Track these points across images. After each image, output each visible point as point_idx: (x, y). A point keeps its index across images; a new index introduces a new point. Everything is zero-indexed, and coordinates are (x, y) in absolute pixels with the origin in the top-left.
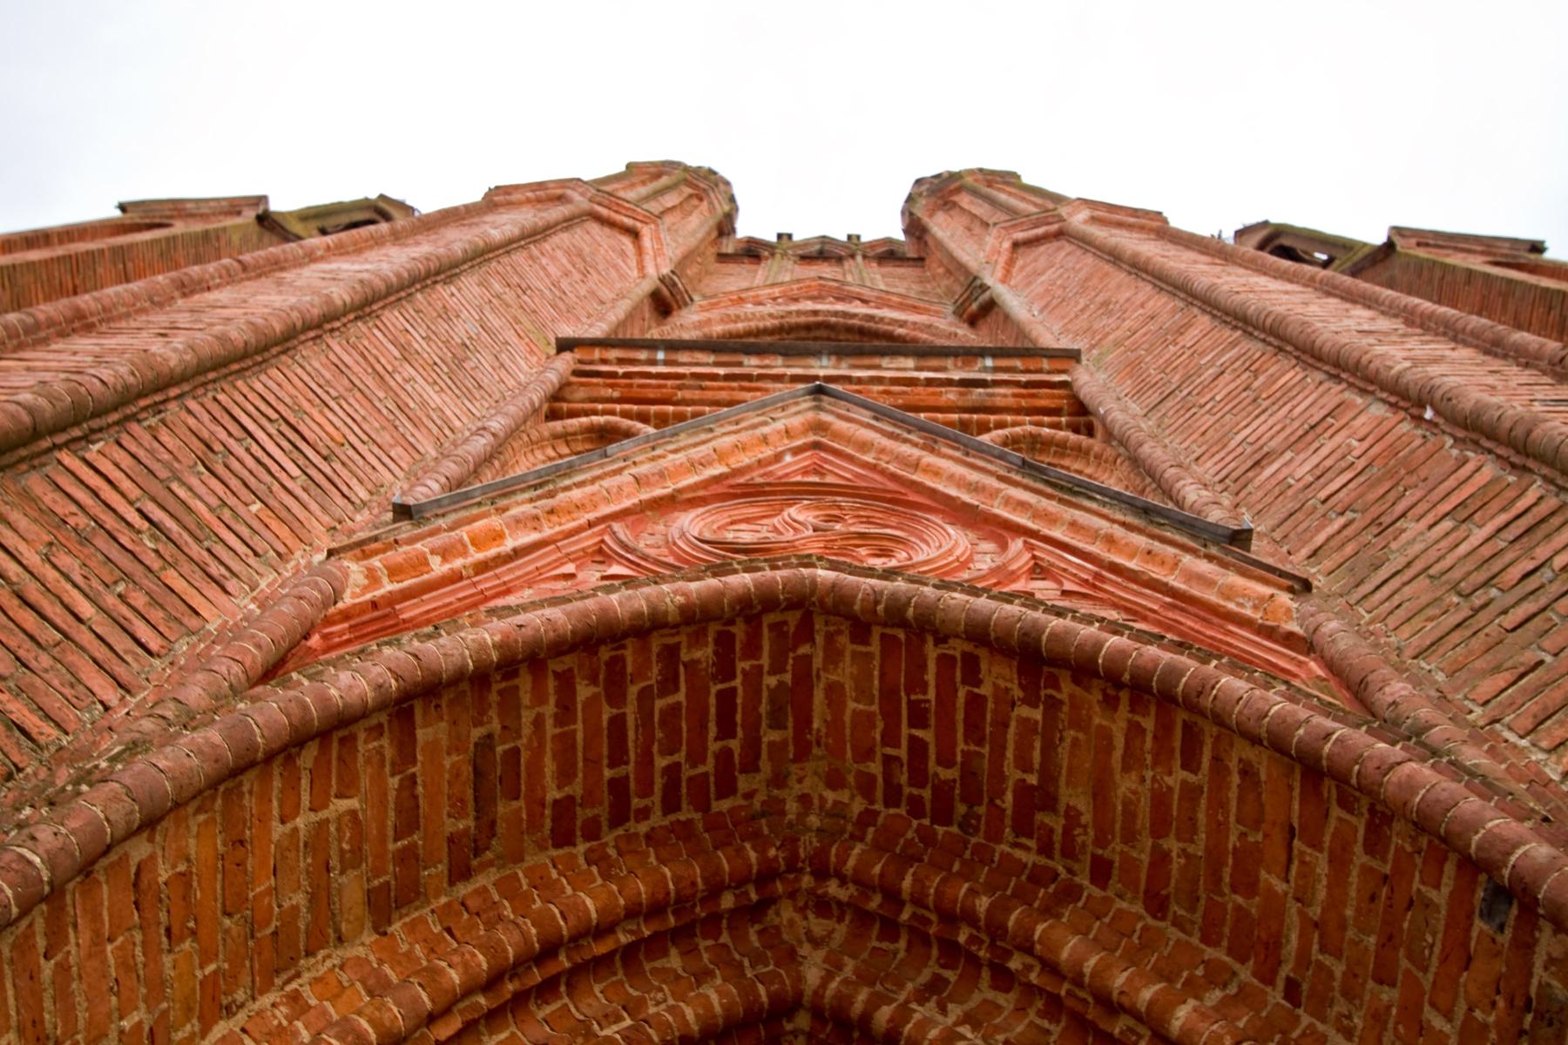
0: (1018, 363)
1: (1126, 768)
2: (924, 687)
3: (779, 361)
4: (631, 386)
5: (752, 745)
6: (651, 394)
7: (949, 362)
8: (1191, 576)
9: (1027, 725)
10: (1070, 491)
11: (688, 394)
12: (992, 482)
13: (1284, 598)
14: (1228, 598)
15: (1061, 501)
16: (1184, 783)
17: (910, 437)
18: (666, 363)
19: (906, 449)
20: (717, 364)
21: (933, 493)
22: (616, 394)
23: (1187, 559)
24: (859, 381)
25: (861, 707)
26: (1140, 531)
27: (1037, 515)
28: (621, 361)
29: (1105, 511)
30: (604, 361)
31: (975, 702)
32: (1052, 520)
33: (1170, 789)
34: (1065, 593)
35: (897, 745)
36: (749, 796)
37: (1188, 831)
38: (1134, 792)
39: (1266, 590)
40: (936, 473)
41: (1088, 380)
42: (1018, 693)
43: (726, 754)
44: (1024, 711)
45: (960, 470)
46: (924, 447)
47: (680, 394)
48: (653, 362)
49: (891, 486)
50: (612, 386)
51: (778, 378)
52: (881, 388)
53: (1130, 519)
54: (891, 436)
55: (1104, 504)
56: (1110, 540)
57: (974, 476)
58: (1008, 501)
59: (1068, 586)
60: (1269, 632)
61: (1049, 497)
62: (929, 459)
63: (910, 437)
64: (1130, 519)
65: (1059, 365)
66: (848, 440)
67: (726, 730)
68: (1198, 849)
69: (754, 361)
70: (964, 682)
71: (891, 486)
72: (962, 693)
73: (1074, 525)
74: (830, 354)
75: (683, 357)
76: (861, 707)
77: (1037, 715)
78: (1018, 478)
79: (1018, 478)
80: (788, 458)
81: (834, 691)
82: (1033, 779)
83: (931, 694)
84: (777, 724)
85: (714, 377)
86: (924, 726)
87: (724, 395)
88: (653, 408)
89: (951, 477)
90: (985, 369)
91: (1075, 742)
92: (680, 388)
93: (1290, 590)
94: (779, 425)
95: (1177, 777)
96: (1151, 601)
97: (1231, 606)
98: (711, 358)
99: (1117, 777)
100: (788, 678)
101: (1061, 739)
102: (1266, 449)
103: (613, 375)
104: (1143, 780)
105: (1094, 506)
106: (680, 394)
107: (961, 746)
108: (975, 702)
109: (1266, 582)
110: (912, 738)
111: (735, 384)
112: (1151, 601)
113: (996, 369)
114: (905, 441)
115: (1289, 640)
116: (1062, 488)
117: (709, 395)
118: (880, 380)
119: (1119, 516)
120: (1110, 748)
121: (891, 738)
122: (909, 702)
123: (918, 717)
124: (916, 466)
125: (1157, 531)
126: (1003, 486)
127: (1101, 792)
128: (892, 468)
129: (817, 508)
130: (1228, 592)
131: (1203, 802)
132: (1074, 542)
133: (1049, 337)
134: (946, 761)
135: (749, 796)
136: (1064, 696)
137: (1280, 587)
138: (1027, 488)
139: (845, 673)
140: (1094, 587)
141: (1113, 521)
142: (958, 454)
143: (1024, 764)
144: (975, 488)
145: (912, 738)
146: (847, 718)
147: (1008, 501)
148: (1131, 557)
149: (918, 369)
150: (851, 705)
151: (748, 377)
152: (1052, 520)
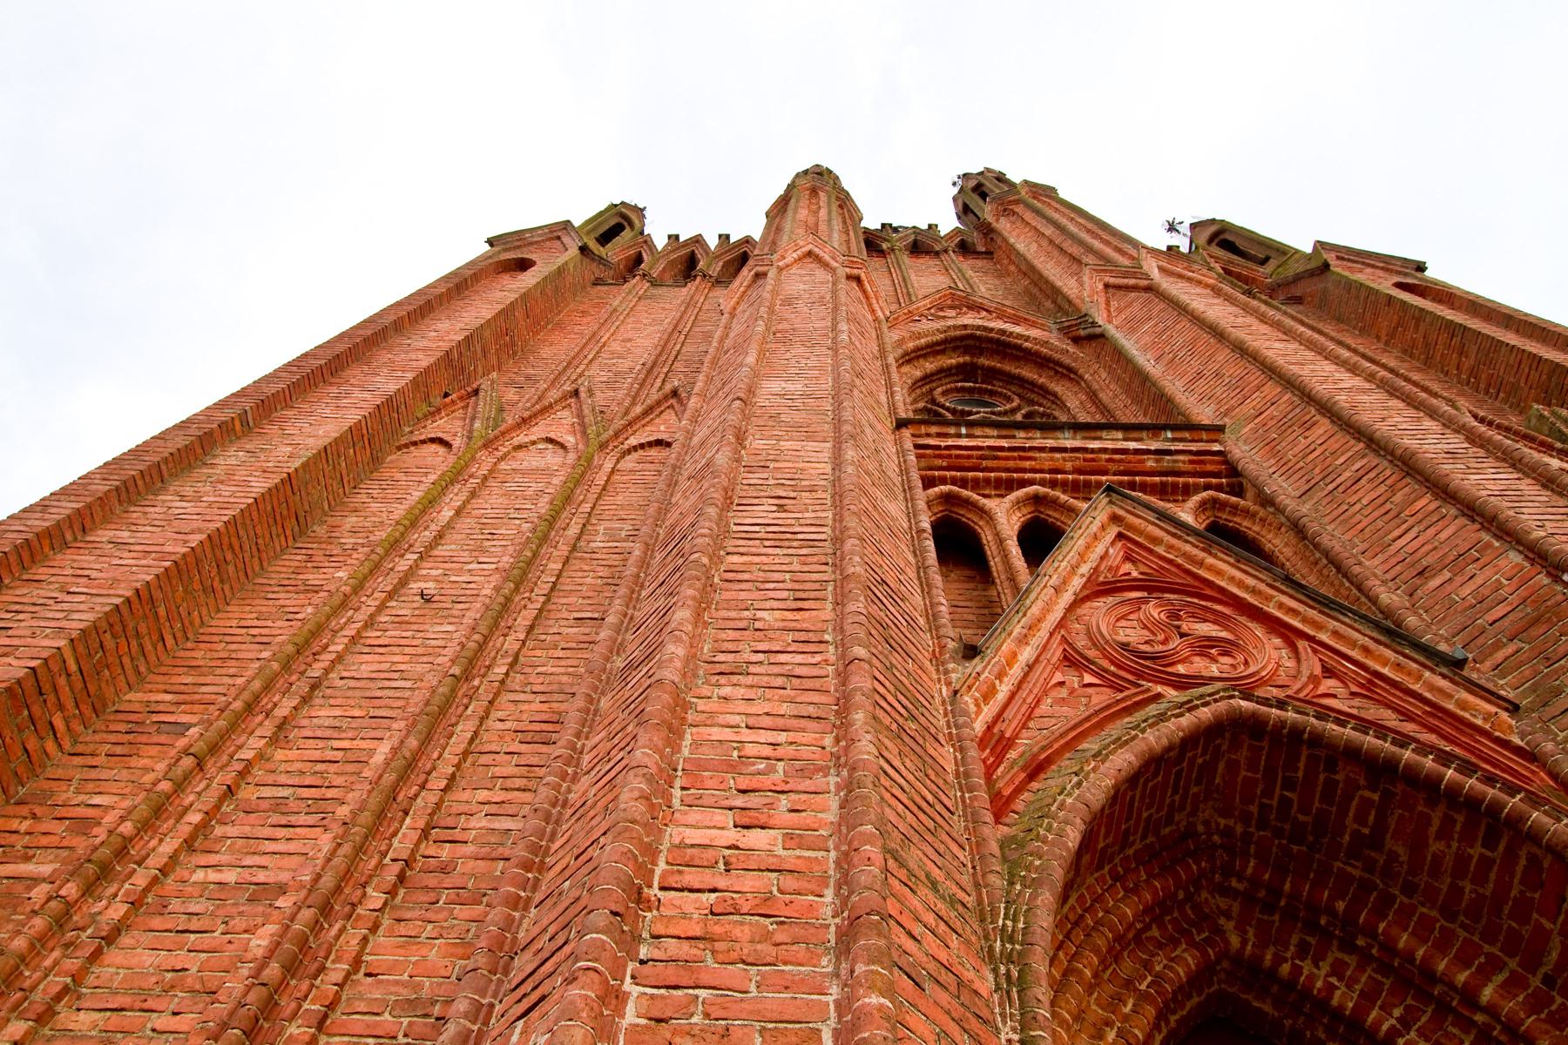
0: (1187, 435)
1: (1438, 837)
2: (1296, 769)
3: (1038, 434)
4: (950, 456)
5: (1184, 798)
6: (966, 463)
7: (1144, 434)
8: (1432, 688)
9: (1366, 802)
10: (1327, 606)
11: (990, 463)
12: (1263, 587)
13: (1504, 715)
14: (1463, 709)
15: (1320, 612)
16: (1482, 856)
17: (1189, 538)
18: (968, 436)
19: (1188, 548)
20: (999, 437)
21: (1222, 590)
22: (945, 464)
23: (1427, 674)
24: (1093, 451)
25: (1249, 774)
26: (1386, 646)
27: (1305, 620)
28: (939, 435)
29: (1356, 625)
30: (928, 435)
31: (1330, 785)
32: (1319, 627)
33: (1471, 857)
34: (1353, 694)
35: (1272, 799)
36: (1178, 823)
37: (1481, 879)
38: (1442, 852)
39: (1493, 709)
40: (1219, 573)
41: (1242, 449)
42: (1362, 782)
43: (1173, 802)
44: (1367, 793)
45: (1238, 574)
46: (1203, 550)
47: (985, 463)
48: (959, 436)
49: (1190, 581)
50: (940, 457)
51: (1041, 449)
52: (1107, 456)
53: (1375, 635)
54: (1174, 535)
55: (1355, 621)
56: (1366, 650)
57: (1251, 582)
58: (1281, 606)
59: (1355, 689)
60: (1505, 744)
61: (1314, 608)
62: (1210, 560)
63: (1189, 538)
64: (1375, 635)
65: (1213, 436)
66: (1140, 533)
67: (1175, 792)
68: (1488, 890)
69: (1022, 434)
70: (1324, 771)
71: (1190, 581)
72: (1322, 777)
73: (1335, 633)
74: (1069, 428)
75: (978, 432)
76: (1249, 774)
77: (1376, 797)
78: (1283, 588)
79: (1283, 588)
80: (1111, 551)
81: (1233, 766)
82: (1366, 831)
83: (1300, 774)
84: (1198, 783)
85: (1001, 449)
86: (1292, 790)
87: (1011, 464)
88: (970, 474)
89: (1232, 579)
90: (1167, 440)
91: (1401, 817)
92: (982, 458)
93: (1506, 710)
94: (1097, 523)
95: (1476, 851)
96: (1417, 709)
97: (1467, 715)
98: (995, 433)
99: (1431, 841)
100: (1208, 757)
101: (1392, 813)
102: (1425, 563)
103: (938, 447)
104: (1449, 847)
105: (1347, 620)
106: (985, 463)
107: (1317, 804)
108: (1330, 785)
109: (1489, 701)
110: (1282, 797)
111: (1016, 454)
112: (1417, 709)
113: (1174, 440)
114: (1187, 541)
115: (1518, 750)
116: (1320, 602)
117: (1002, 463)
118: (1105, 450)
119: (1368, 632)
120: (1429, 824)
121: (1268, 793)
122: (1284, 778)
123: (1289, 784)
124: (1201, 564)
125: (1400, 649)
126: (1275, 593)
127: (1417, 846)
128: (1179, 561)
129: (1161, 606)
130: (1463, 705)
131: (1495, 869)
132: (1338, 646)
133: (1205, 414)
134: (1305, 810)
135: (1178, 823)
136: (1398, 791)
137: (1499, 706)
138: (1291, 597)
139: (1243, 755)
140: (1369, 690)
141: (1365, 635)
142: (1232, 560)
143: (1361, 818)
144: (1254, 591)
145: (1282, 797)
146: (1239, 780)
147: (1281, 606)
148: (1385, 664)
149: (1125, 439)
150: (1244, 773)
151: (1023, 449)
152: (1319, 627)
